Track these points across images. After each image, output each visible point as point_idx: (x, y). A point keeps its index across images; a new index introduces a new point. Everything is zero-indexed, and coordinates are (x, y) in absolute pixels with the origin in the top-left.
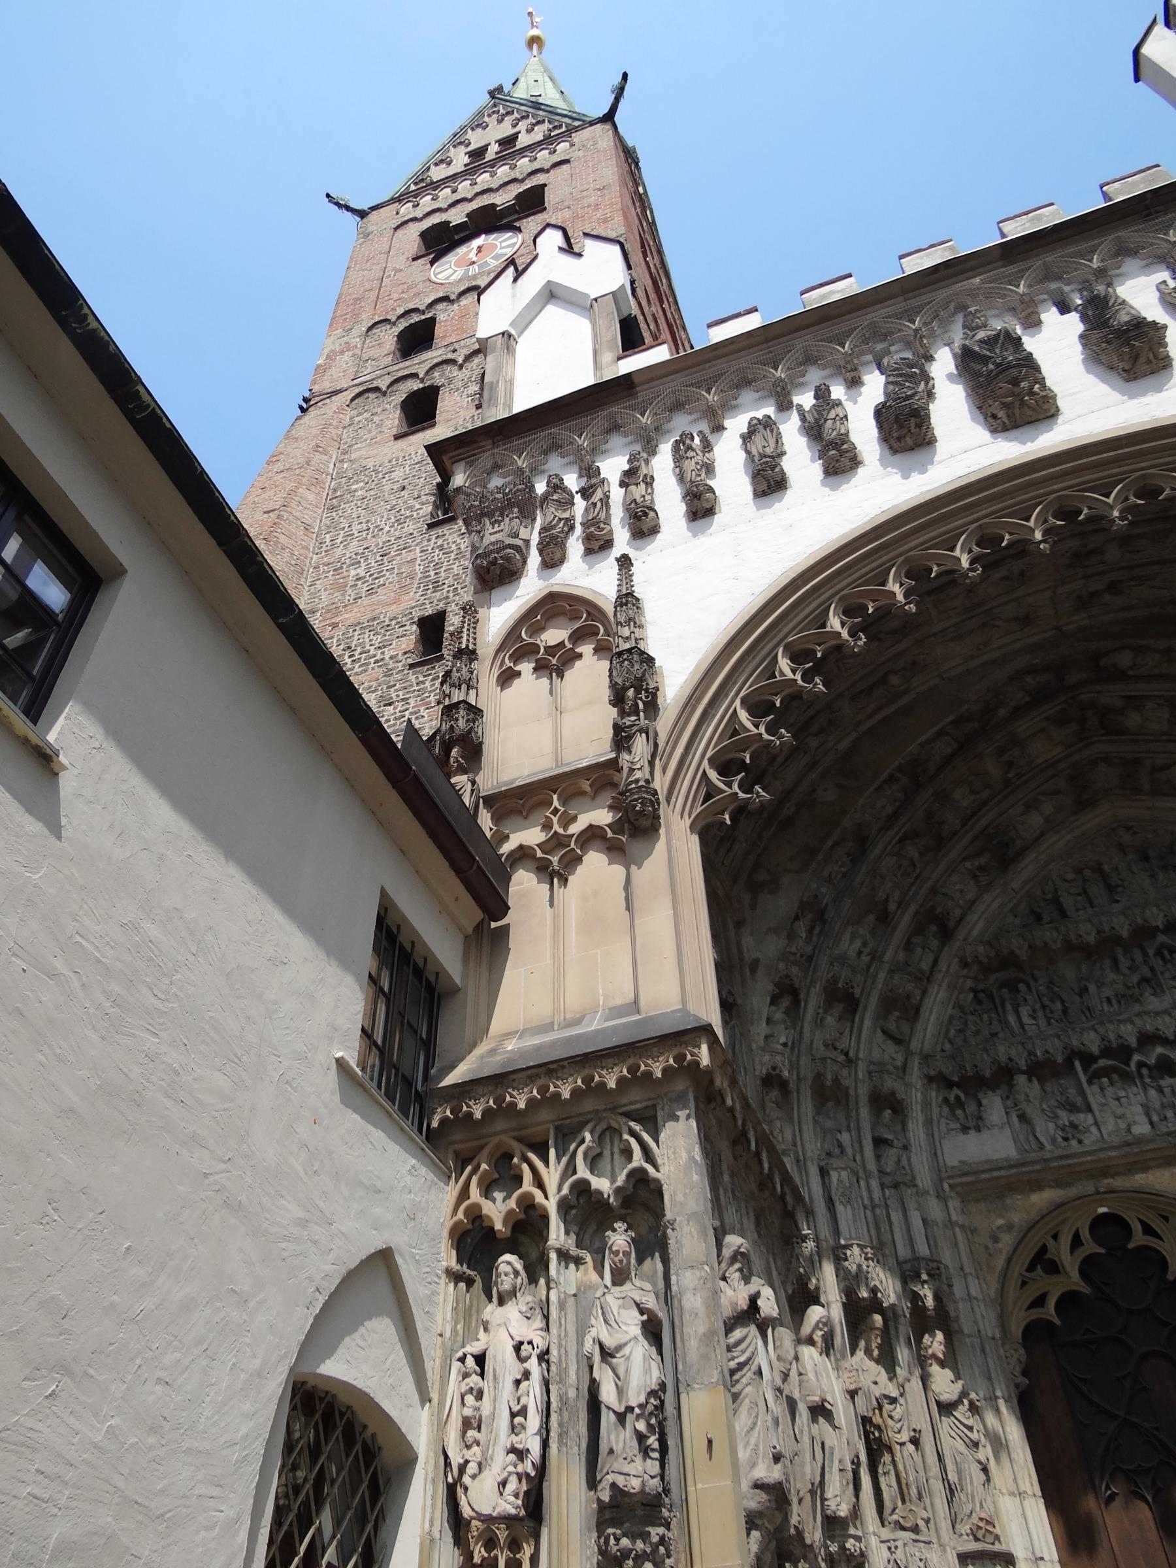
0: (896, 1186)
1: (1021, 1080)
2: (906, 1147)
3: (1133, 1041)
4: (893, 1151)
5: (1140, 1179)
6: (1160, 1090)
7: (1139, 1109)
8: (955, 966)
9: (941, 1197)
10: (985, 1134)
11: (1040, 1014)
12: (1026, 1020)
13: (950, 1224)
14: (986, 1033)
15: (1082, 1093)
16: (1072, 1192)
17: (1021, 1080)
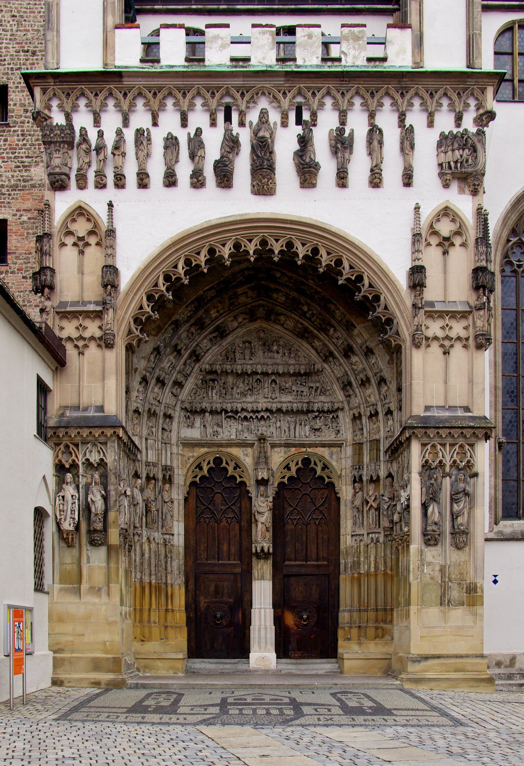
0: (165, 443)
1: (207, 414)
2: (171, 431)
3: (240, 410)
4: (167, 433)
5: (229, 450)
6: (242, 425)
7: (234, 430)
8: (198, 371)
9: (177, 446)
10: (193, 430)
11: (218, 394)
12: (214, 395)
13: (178, 454)
14: (201, 396)
15: (222, 422)
16: (211, 450)
17: (207, 414)
